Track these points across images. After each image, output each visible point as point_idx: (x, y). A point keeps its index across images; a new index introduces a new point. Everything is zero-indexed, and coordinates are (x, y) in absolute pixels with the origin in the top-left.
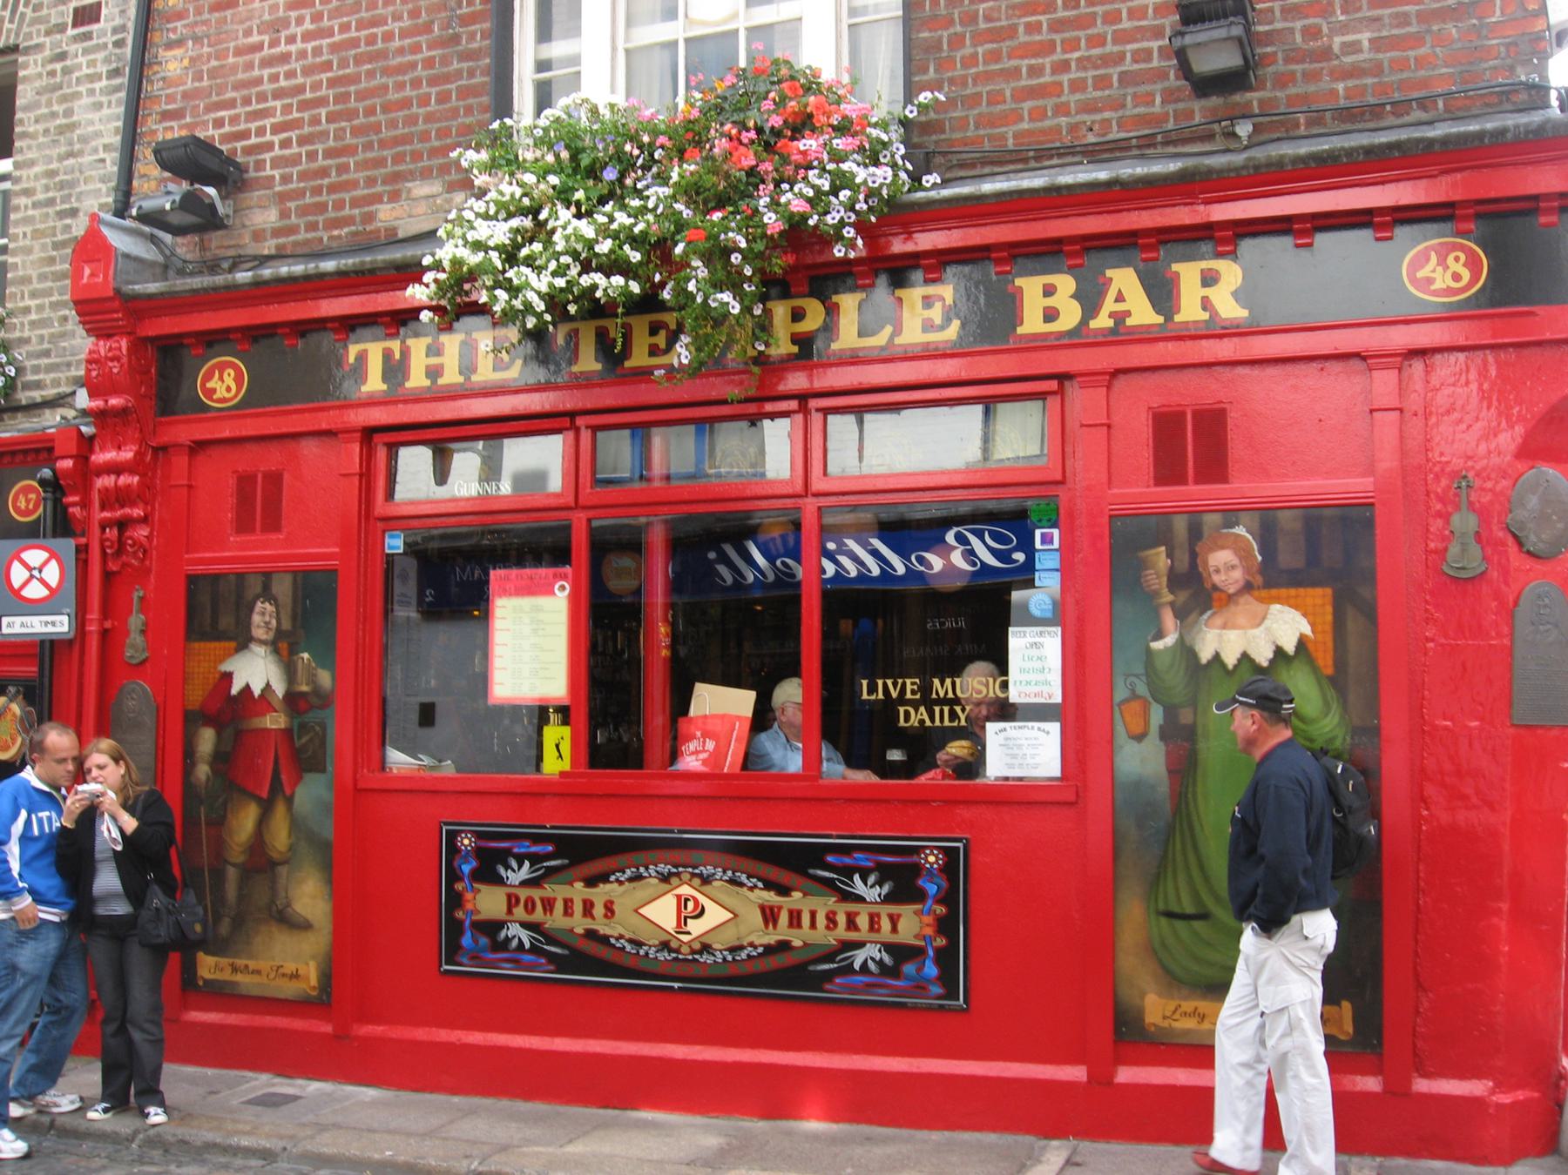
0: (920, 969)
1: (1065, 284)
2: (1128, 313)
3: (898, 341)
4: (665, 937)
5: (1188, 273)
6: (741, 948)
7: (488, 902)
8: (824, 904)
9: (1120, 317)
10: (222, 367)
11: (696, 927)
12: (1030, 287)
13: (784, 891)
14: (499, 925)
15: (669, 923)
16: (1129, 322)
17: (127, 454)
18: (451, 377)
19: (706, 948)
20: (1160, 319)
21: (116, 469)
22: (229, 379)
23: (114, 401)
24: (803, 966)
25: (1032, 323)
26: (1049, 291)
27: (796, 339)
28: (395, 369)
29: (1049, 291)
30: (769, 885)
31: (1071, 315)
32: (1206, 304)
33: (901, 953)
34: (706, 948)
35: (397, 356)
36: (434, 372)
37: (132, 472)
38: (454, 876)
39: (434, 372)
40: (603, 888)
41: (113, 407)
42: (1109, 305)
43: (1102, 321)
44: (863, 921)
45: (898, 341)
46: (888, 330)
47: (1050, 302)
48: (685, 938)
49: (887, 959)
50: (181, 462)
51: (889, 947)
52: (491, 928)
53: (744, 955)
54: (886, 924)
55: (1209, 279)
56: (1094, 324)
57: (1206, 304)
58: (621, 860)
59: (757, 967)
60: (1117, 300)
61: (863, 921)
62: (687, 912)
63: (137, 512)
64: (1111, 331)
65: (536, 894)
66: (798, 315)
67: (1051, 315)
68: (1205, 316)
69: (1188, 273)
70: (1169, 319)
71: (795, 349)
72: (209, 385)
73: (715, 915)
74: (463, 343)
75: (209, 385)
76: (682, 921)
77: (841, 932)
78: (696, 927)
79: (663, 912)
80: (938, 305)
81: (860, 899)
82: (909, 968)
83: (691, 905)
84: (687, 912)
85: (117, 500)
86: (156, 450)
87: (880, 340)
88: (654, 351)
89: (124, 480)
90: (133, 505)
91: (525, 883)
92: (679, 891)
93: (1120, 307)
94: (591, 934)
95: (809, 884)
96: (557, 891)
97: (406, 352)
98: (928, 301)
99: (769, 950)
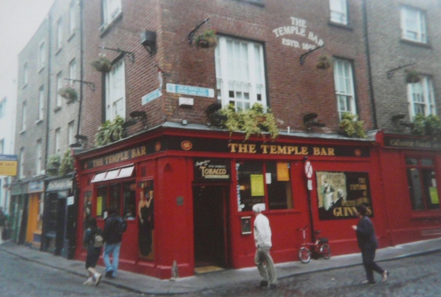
9: (323, 153)
25: (315, 154)
36: (243, 150)
39: (243, 150)
42: (322, 152)
66: (291, 149)
67: (317, 152)
87: (300, 153)
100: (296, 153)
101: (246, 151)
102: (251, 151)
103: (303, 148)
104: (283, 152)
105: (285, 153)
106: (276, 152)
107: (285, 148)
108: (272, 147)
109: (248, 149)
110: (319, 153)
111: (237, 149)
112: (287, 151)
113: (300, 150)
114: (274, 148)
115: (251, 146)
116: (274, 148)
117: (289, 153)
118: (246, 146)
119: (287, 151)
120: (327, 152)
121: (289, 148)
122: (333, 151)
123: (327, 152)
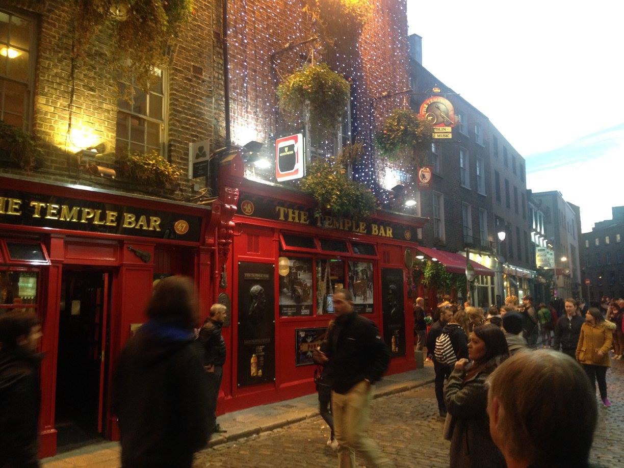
7: (304, 347)
12: (373, 226)
14: (306, 353)
22: (249, 208)
25: (373, 233)
27: (348, 228)
36: (293, 218)
38: (298, 343)
39: (293, 218)
42: (381, 232)
52: (305, 353)
65: (313, 344)
67: (375, 232)
71: (348, 229)
88: (329, 225)
91: (311, 342)
101: (297, 220)
102: (302, 221)
103: (361, 224)
104: (339, 226)
105: (341, 228)
109: (299, 219)
110: (377, 233)
111: (286, 216)
115: (302, 213)
117: (346, 229)
118: (297, 212)
123: (386, 233)
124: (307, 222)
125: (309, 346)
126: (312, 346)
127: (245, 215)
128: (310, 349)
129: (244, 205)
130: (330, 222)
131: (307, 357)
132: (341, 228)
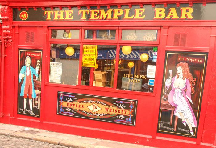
0: (128, 119)
1: (163, 10)
2: (173, 16)
3: (135, 18)
4: (91, 111)
5: (184, 9)
6: (102, 114)
8: (115, 108)
9: (171, 17)
10: (24, 13)
11: (96, 110)
12: (157, 10)
13: (109, 106)
15: (92, 109)
16: (173, 18)
17: (8, 27)
18: (62, 18)
19: (97, 114)
20: (178, 18)
21: (6, 29)
23: (6, 17)
24: (111, 117)
25: (157, 17)
26: (160, 11)
27: (118, 16)
28: (53, 16)
29: (160, 11)
30: (107, 105)
31: (163, 15)
32: (186, 15)
33: (126, 117)
34: (97, 114)
35: (53, 14)
36: (59, 17)
37: (9, 30)
39: (59, 17)
40: (82, 103)
41: (5, 19)
42: (170, 14)
43: (169, 17)
44: (121, 112)
45: (135, 18)
46: (133, 16)
47: (161, 13)
48: (94, 112)
49: (124, 118)
50: (17, 29)
51: (124, 116)
53: (102, 115)
54: (124, 112)
55: (187, 11)
56: (167, 17)
57: (186, 15)
58: (85, 99)
59: (104, 117)
60: (171, 14)
61: (121, 112)
62: (95, 108)
63: (10, 37)
64: (170, 19)
66: (119, 12)
68: (186, 17)
69: (184, 9)
70: (180, 17)
71: (118, 18)
72: (22, 16)
73: (98, 109)
74: (64, 12)
75: (22, 16)
76: (93, 109)
77: (117, 113)
78: (96, 110)
79: (91, 108)
80: (142, 12)
81: (120, 108)
82: (127, 119)
83: (95, 107)
84: (95, 108)
85: (6, 35)
86: (13, 27)
87: (132, 17)
89: (8, 31)
90: (9, 36)
92: (93, 105)
93: (172, 15)
94: (80, 110)
95: (113, 105)
96: (75, 103)
97: (54, 13)
98: (140, 12)
99: (106, 115)
100: (127, 17)
102: (67, 18)
104: (107, 16)
106: (97, 18)
107: (110, 11)
108: (93, 11)
109: (64, 17)
112: (113, 15)
113: (132, 13)
114: (95, 12)
116: (95, 12)
117: (116, 17)
119: (113, 15)
120: (179, 13)
121: (116, 11)
122: (191, 10)
123: (179, 13)
124: (72, 18)
125: (68, 104)
126: (71, 104)
127: (22, 20)
128: (69, 106)
129: (21, 14)
130: (96, 14)
131: (66, 111)
132: (109, 17)
